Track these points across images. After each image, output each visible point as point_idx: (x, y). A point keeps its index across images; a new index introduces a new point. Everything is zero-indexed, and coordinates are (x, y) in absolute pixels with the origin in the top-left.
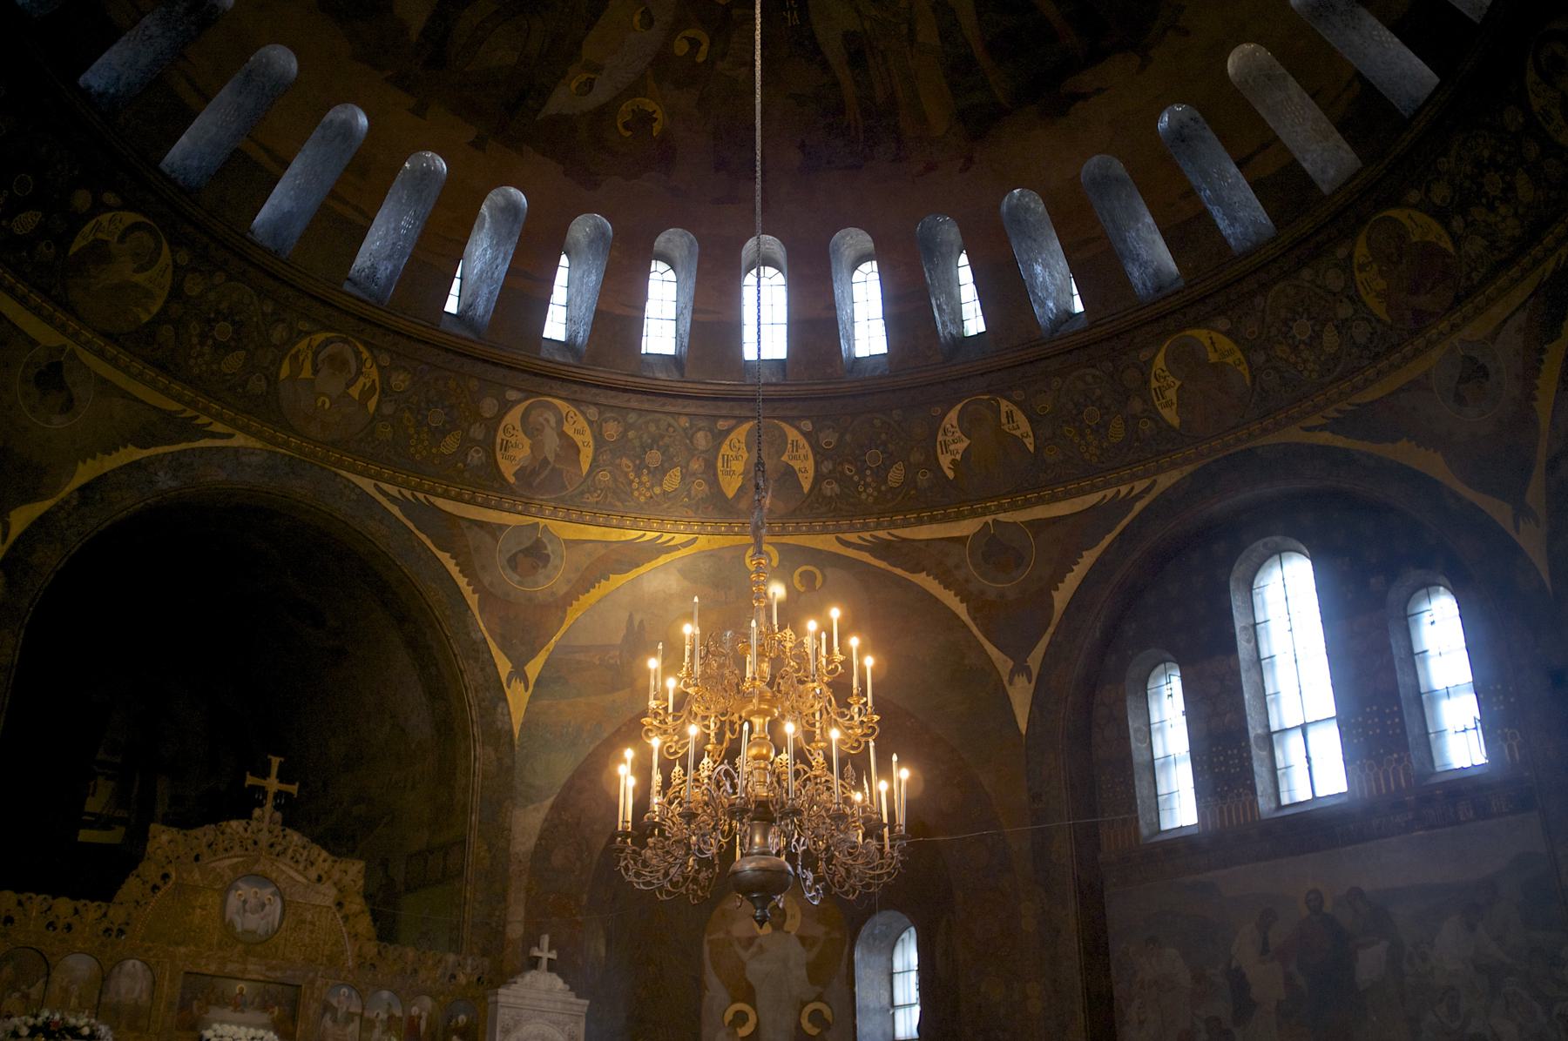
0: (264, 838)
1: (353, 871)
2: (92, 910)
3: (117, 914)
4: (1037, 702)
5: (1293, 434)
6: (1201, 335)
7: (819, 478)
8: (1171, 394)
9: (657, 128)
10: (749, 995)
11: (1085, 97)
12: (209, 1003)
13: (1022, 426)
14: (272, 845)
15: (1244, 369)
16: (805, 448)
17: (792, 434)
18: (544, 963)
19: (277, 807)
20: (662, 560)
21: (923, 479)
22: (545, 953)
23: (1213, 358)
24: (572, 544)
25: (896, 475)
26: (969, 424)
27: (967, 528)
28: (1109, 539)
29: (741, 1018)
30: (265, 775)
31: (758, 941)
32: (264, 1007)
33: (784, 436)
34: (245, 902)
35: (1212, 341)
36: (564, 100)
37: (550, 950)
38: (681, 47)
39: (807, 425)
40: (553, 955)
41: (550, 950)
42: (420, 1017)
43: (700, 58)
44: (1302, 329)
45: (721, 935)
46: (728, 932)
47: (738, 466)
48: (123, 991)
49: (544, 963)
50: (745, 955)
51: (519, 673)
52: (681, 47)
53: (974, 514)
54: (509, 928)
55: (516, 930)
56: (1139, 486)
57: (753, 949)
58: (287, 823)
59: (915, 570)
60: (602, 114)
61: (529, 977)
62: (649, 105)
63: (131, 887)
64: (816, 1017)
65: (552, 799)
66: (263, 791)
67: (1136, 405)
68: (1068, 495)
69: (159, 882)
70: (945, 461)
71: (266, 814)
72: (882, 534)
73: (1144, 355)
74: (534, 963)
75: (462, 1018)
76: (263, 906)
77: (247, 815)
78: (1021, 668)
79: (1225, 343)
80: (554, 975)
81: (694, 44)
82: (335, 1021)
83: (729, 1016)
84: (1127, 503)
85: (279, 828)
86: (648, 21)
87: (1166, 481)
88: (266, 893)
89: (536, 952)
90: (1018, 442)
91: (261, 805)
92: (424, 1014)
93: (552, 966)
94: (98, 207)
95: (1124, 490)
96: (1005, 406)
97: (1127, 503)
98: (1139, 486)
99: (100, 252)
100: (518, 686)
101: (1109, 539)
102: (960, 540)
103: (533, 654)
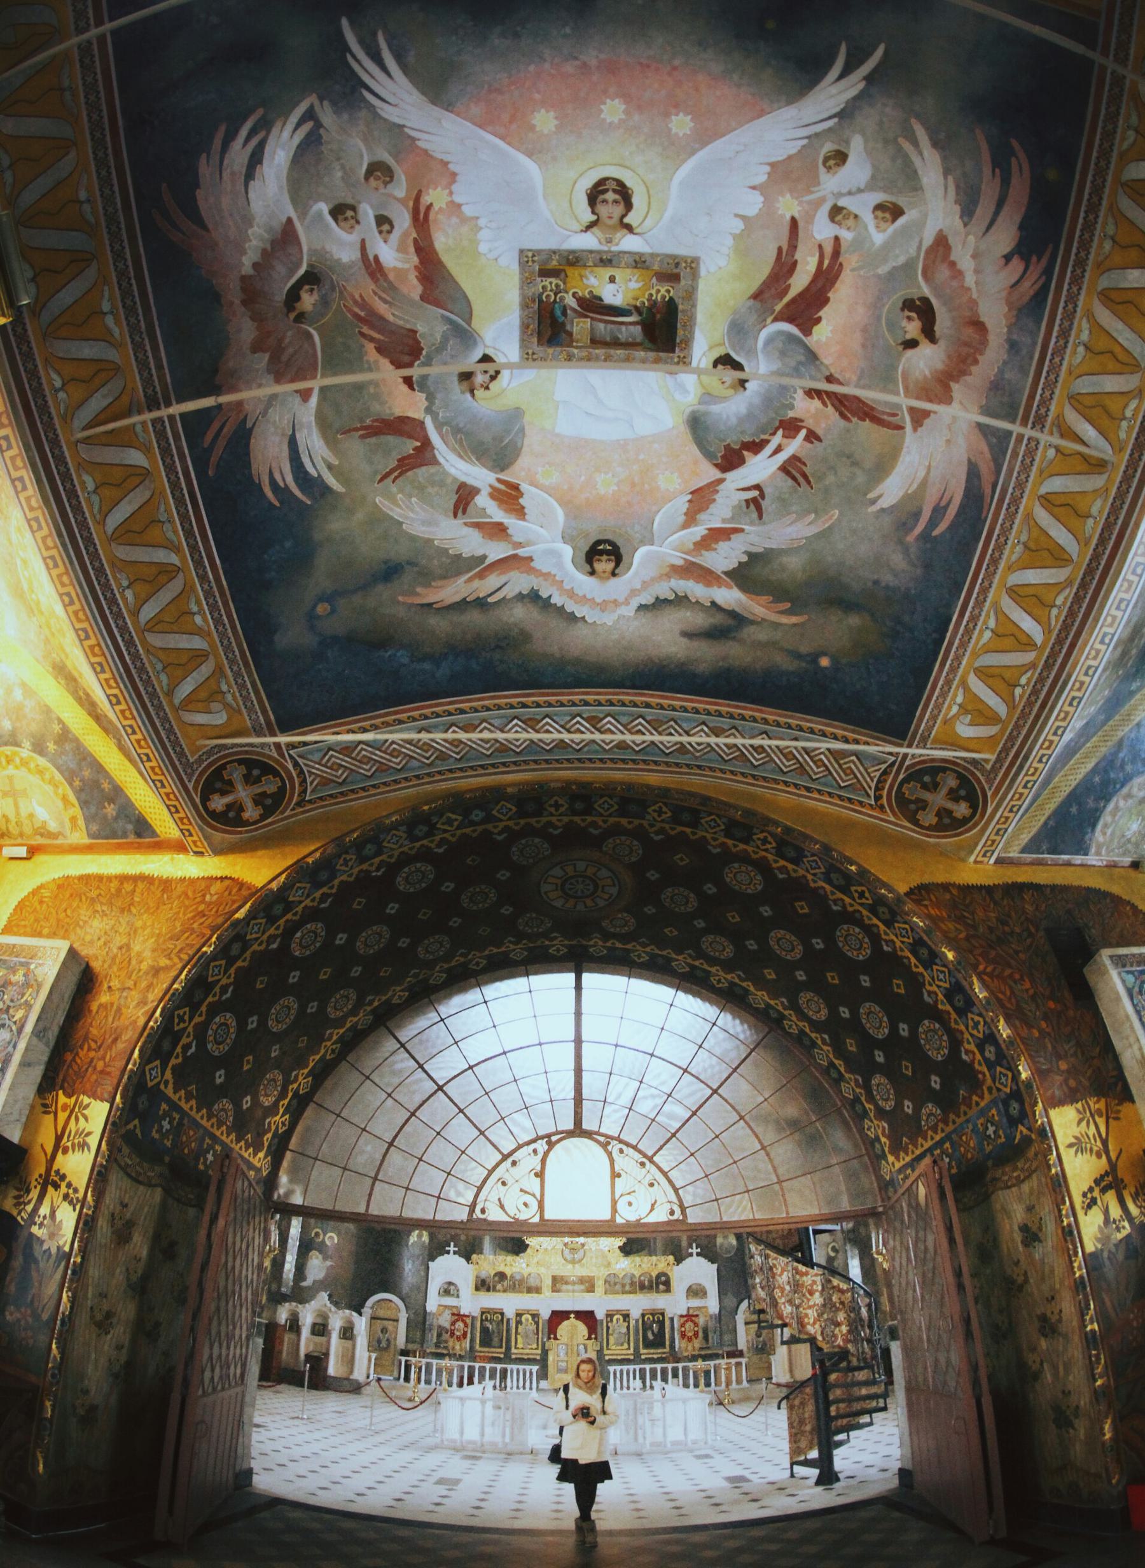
22: (694, 1251)
64: (834, 1249)
74: (691, 1255)
93: (698, 1254)
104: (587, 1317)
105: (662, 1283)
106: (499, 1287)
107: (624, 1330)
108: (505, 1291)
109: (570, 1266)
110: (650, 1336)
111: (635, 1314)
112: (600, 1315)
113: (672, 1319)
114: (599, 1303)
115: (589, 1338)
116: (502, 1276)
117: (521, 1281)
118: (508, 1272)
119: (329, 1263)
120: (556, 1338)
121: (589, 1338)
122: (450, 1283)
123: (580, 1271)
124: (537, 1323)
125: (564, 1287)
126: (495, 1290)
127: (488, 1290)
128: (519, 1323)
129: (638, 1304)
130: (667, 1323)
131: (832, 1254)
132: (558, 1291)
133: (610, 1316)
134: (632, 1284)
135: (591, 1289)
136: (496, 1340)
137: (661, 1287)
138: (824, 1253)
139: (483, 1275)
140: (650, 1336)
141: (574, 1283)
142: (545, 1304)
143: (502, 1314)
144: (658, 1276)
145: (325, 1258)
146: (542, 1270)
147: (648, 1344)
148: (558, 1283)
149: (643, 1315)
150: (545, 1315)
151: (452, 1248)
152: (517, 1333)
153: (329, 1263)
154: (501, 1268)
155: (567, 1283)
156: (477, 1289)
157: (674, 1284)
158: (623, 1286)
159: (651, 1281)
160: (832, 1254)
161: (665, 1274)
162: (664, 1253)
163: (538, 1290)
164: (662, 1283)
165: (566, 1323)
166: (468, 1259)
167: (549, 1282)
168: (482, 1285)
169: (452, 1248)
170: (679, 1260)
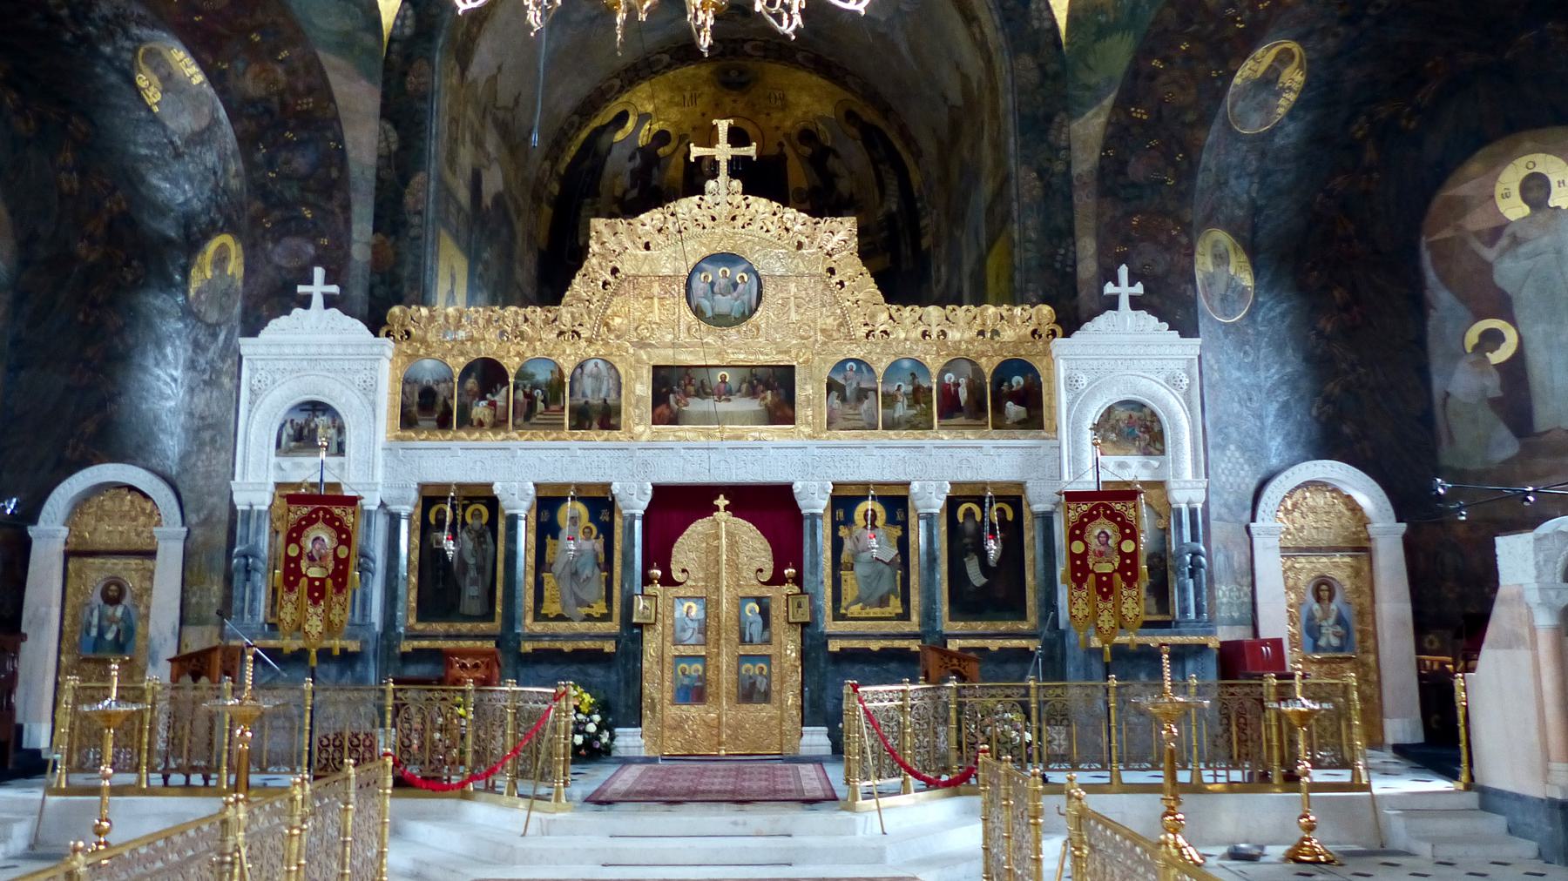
0: (723, 211)
1: (841, 232)
2: (538, 313)
3: (565, 313)
10: (1503, 306)
12: (687, 395)
14: (734, 218)
18: (1124, 302)
19: (733, 174)
22: (1124, 289)
29: (1492, 339)
30: (711, 141)
31: (1508, 231)
32: (753, 393)
34: (712, 284)
37: (1131, 284)
40: (1139, 289)
41: (1131, 284)
42: (957, 385)
45: (1447, 233)
46: (1460, 228)
48: (589, 392)
49: (1124, 302)
50: (1489, 254)
54: (1079, 268)
55: (1087, 268)
57: (1504, 242)
58: (747, 191)
61: (1102, 321)
65: (1112, 96)
66: (715, 163)
69: (610, 278)
74: (1112, 303)
75: (1018, 381)
76: (735, 285)
77: (700, 191)
80: (1143, 313)
82: (844, 399)
83: (1472, 336)
85: (739, 197)
88: (738, 274)
89: (1110, 288)
91: (714, 175)
92: (963, 381)
93: (1136, 303)
104: (768, 505)
105: (1013, 397)
106: (480, 410)
107: (891, 552)
108: (498, 424)
110: (977, 578)
111: (930, 497)
112: (814, 499)
113: (1047, 519)
114: (808, 459)
115: (777, 579)
116: (488, 374)
117: (554, 389)
120: (667, 580)
121: (777, 579)
122: (315, 407)
124: (607, 530)
125: (696, 406)
126: (466, 421)
127: (444, 423)
128: (546, 529)
129: (940, 465)
130: (1031, 535)
132: (674, 420)
133: (844, 501)
134: (919, 395)
135: (782, 412)
136: (472, 592)
137: (1012, 408)
139: (428, 369)
140: (977, 578)
141: (725, 393)
142: (635, 462)
143: (493, 503)
144: (1006, 370)
147: (966, 603)
148: (672, 389)
149: (952, 503)
150: (634, 500)
151: (318, 287)
152: (541, 564)
154: (490, 347)
155: (702, 392)
156: (408, 421)
157: (1060, 401)
158: (890, 400)
159: (976, 390)
161: (1025, 368)
163: (605, 417)
164: (1013, 397)
165: (699, 527)
166: (376, 323)
167: (642, 388)
168: (425, 409)
169: (318, 287)
170: (1070, 323)
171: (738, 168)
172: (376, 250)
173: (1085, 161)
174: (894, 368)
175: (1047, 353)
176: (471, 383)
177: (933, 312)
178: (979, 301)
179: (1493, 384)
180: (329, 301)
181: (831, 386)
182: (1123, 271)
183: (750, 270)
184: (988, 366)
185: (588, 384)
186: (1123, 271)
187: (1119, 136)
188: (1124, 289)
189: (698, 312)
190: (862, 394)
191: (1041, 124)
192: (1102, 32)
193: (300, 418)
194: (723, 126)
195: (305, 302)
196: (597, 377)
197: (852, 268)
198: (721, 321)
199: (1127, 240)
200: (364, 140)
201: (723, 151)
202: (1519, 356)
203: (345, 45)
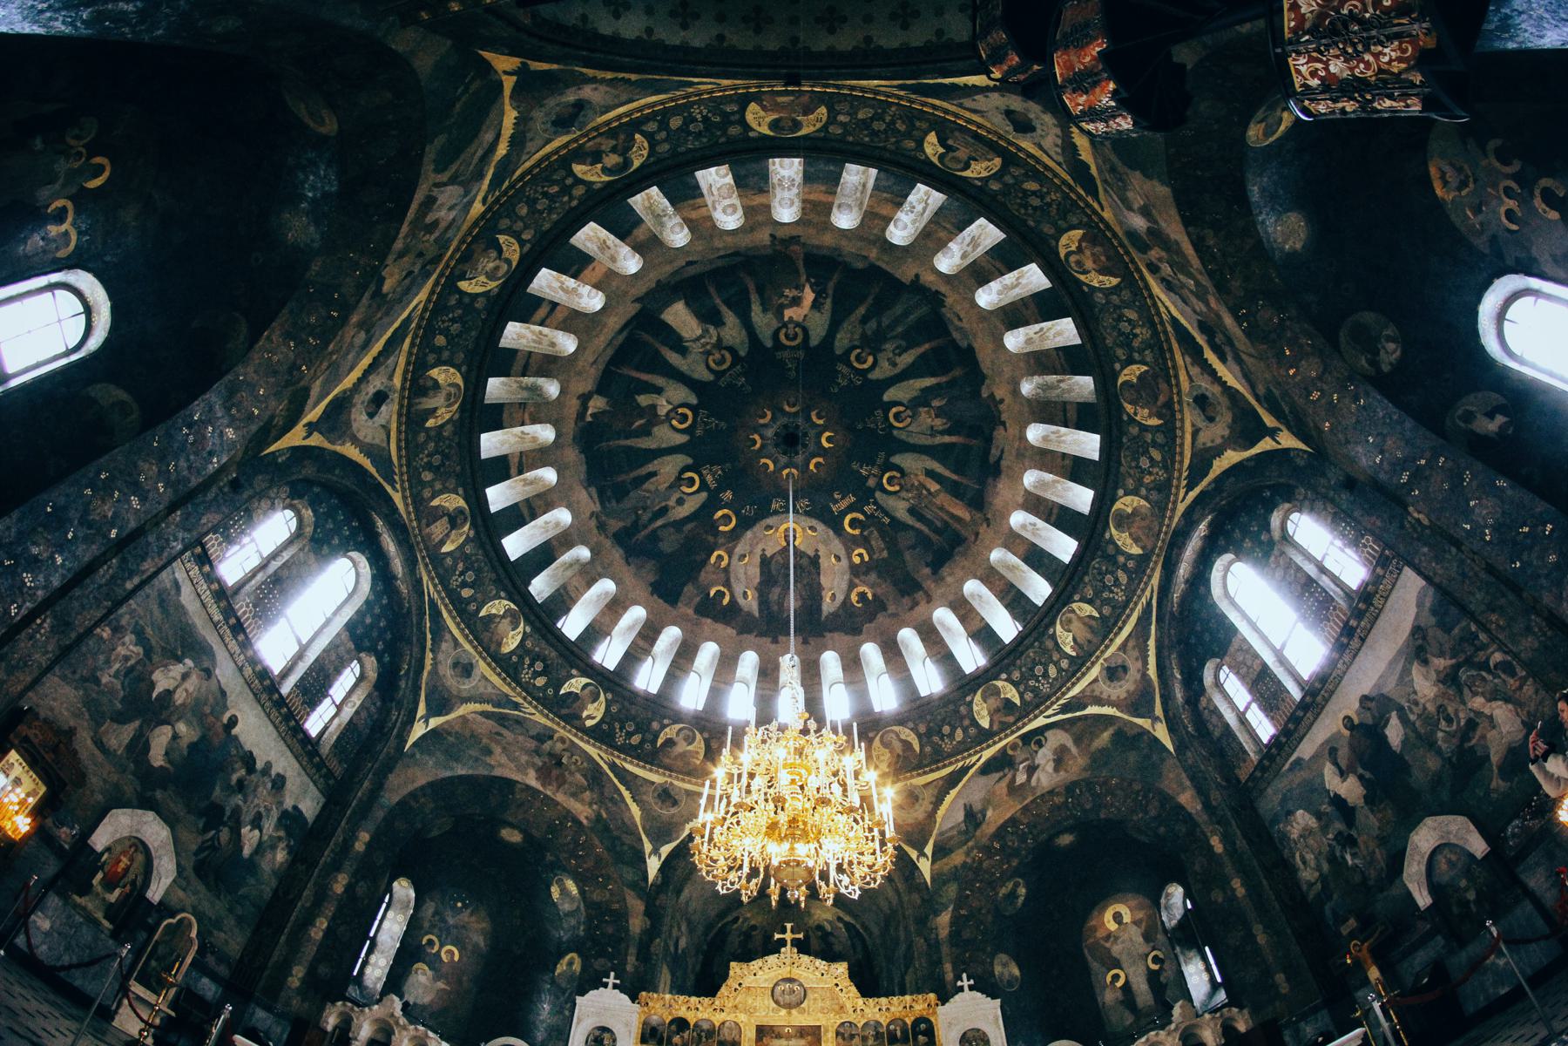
0: (788, 961)
1: (841, 968)
2: (706, 1000)
4: (1172, 730)
5: (1181, 508)
6: (1118, 505)
7: (1021, 695)
8: (1129, 541)
9: (870, 596)
10: (1117, 965)
11: (1000, 458)
13: (1088, 610)
15: (1143, 502)
16: (1009, 687)
17: (999, 684)
20: (972, 771)
21: (1065, 664)
22: (965, 982)
23: (1129, 510)
24: (926, 786)
25: (1052, 671)
26: (1067, 626)
27: (1095, 672)
28: (1153, 627)
29: (1116, 977)
30: (784, 931)
33: (996, 687)
35: (1126, 503)
36: (828, 606)
38: (857, 560)
39: (1004, 676)
43: (867, 558)
44: (1144, 463)
47: (985, 713)
51: (922, 854)
52: (857, 560)
53: (1093, 664)
55: (950, 976)
56: (1148, 593)
59: (1085, 708)
60: (846, 602)
62: (861, 589)
63: (723, 990)
64: (1156, 960)
67: (1121, 559)
68: (1125, 623)
70: (1068, 650)
71: (787, 951)
72: (1062, 702)
73: (1107, 536)
74: (961, 989)
75: (923, 1026)
78: (1155, 719)
79: (1128, 499)
81: (860, 555)
83: (1109, 979)
84: (1149, 604)
86: (838, 558)
87: (1155, 581)
90: (1091, 617)
93: (971, 988)
94: (664, 727)
95: (1144, 600)
96: (1074, 606)
97: (1149, 604)
98: (1148, 593)
99: (670, 743)
100: (923, 860)
101: (1153, 627)
102: (1096, 680)
103: (926, 842)
109: (783, 1012)
118: (692, 1017)
119: (441, 985)
122: (604, 1029)
123: (799, 1019)
131: (1155, 967)
138: (1141, 969)
139: (655, 1019)
141: (788, 1037)
144: (917, 1022)
145: (436, 978)
146: (742, 1018)
151: (611, 980)
153: (441, 985)
154: (682, 1012)
155: (779, 1036)
156: (643, 1040)
160: (1155, 967)
162: (918, 990)
166: (634, 998)
169: (611, 980)
170: (944, 999)
171: (795, 943)
172: (636, 968)
173: (944, 933)
174: (866, 1024)
175: (935, 1013)
176: (673, 1027)
177: (883, 1000)
178: (903, 993)
179: (1119, 994)
180: (615, 986)
181: (838, 1033)
182: (964, 976)
183: (801, 985)
184: (909, 1021)
185: (725, 1031)
186: (964, 976)
187: (956, 921)
188: (965, 982)
189: (777, 1002)
190: (852, 1036)
191: (923, 921)
192: (945, 883)
193: (597, 1033)
194: (789, 926)
195: (606, 985)
196: (730, 1029)
197: (845, 982)
198: (789, 1006)
199: (964, 963)
200: (637, 924)
201: (788, 936)
202: (1127, 982)
203: (634, 886)
